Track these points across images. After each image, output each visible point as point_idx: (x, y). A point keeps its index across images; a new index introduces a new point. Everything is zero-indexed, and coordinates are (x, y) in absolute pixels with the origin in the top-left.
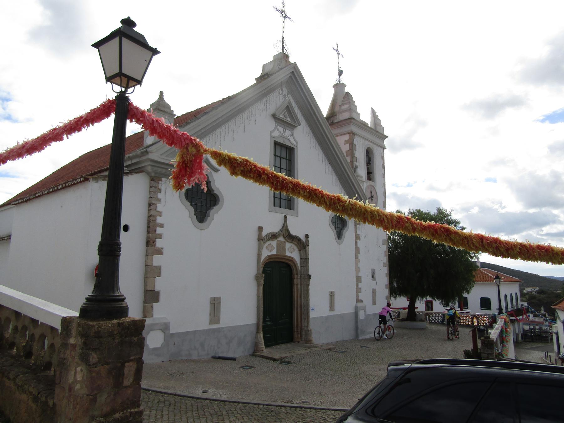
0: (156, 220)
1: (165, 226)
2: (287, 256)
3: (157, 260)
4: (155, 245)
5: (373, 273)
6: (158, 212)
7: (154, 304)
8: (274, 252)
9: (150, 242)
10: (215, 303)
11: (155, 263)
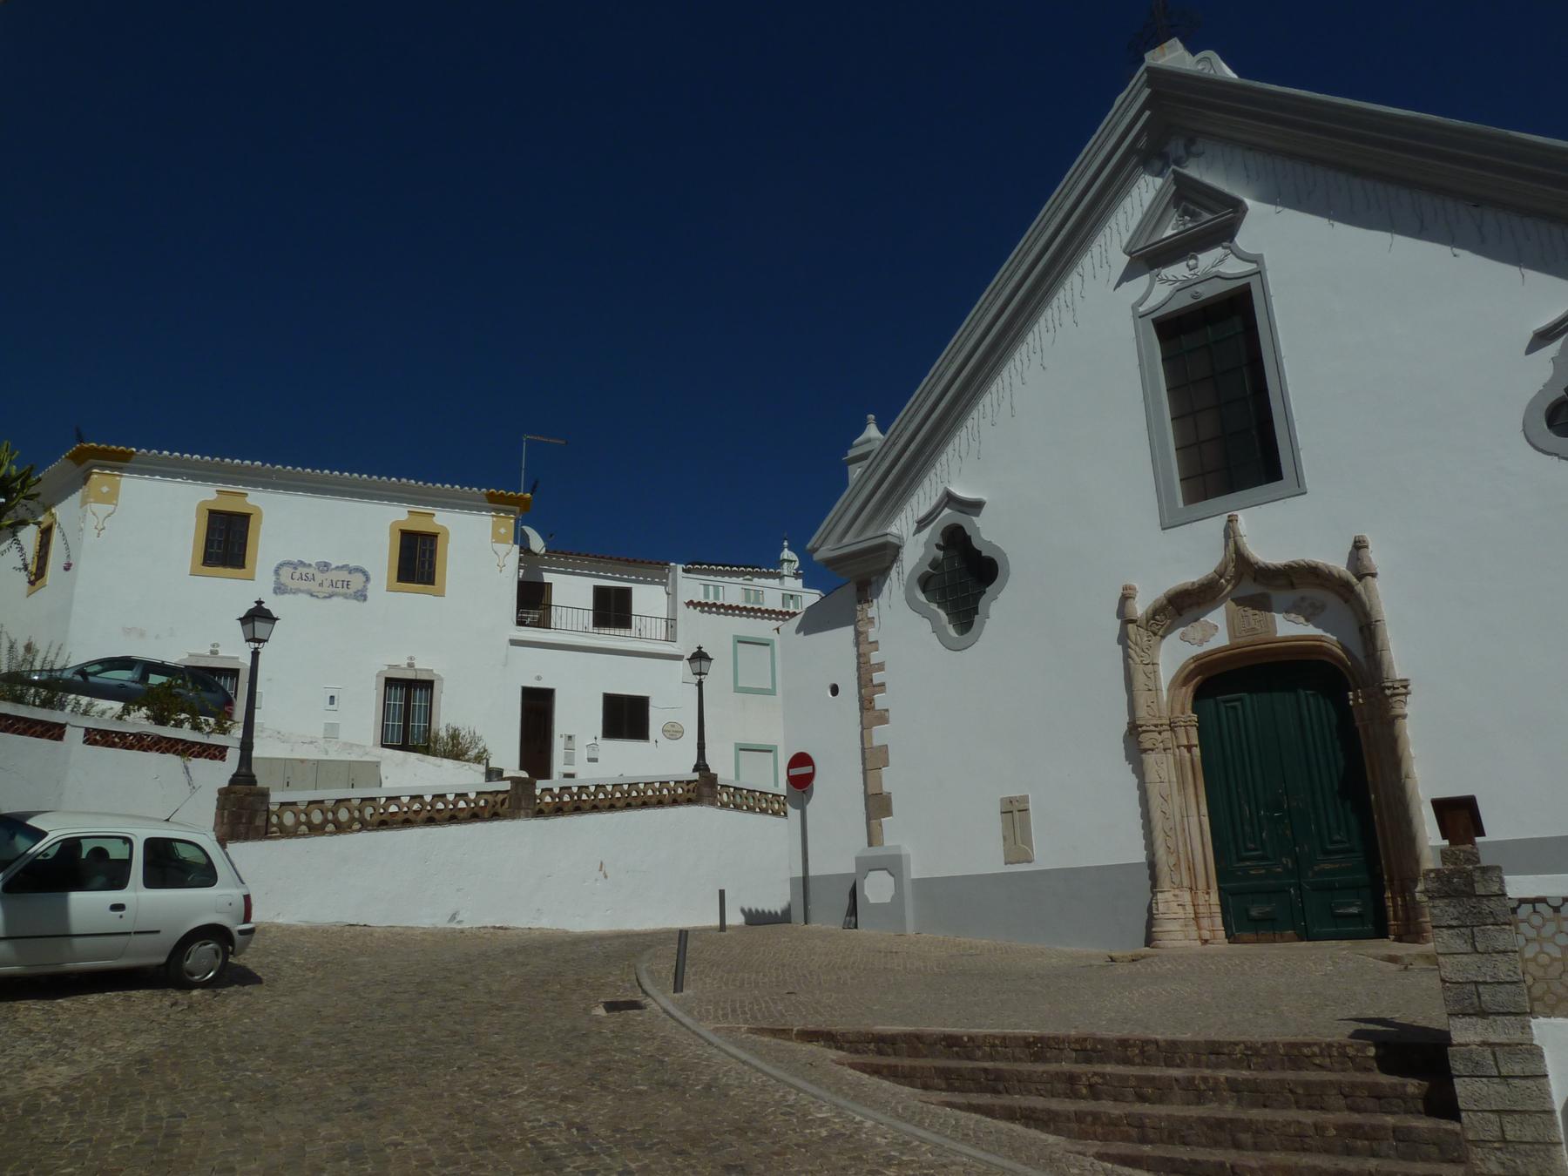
1: (886, 667)
2: (1286, 639)
3: (880, 734)
6: (871, 643)
7: (882, 819)
9: (866, 704)
10: (1015, 812)
11: (877, 742)
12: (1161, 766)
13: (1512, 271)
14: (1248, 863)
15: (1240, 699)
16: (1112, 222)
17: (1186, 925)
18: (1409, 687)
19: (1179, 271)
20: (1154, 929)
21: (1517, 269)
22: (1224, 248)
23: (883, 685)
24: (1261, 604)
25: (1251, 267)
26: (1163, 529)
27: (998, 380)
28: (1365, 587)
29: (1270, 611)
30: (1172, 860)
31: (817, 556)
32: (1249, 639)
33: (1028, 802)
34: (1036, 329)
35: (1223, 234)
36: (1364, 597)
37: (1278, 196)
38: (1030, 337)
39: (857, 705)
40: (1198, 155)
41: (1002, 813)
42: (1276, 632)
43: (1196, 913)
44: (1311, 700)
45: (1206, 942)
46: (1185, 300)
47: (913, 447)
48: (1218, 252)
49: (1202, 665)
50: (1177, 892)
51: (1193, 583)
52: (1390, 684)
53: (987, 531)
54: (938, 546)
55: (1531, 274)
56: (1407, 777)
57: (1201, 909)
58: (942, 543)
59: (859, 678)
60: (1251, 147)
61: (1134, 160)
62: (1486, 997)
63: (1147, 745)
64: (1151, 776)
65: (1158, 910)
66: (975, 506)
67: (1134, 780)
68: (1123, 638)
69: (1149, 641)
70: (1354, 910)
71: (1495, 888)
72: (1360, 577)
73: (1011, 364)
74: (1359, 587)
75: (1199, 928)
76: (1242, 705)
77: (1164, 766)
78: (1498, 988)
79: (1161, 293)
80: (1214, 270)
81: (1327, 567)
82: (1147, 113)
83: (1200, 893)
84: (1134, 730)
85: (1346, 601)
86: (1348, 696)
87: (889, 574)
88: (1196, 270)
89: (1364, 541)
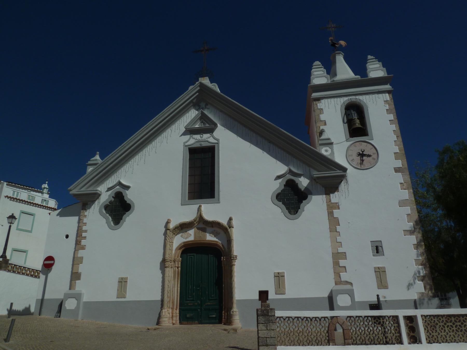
0: (82, 228)
1: (88, 232)
3: (81, 253)
4: (81, 244)
5: (377, 247)
6: (84, 223)
7: (77, 281)
8: (191, 238)
10: (123, 282)
11: (79, 255)
12: (170, 272)
13: (274, 160)
14: (188, 302)
15: (194, 255)
16: (182, 118)
17: (169, 319)
18: (237, 258)
19: (198, 137)
20: (160, 320)
21: (275, 160)
22: (210, 135)
23: (85, 237)
24: (204, 230)
25: (216, 141)
26: (181, 205)
27: (142, 153)
28: (231, 230)
29: (206, 232)
30: (168, 300)
31: (71, 192)
32: (199, 239)
33: (128, 279)
34: (156, 141)
35: (211, 131)
36: (230, 233)
37: (226, 126)
38: (153, 143)
39: (74, 242)
40: (208, 109)
41: (118, 282)
42: (206, 238)
43: (172, 316)
44: (212, 258)
45: (174, 324)
46: (198, 145)
47: (111, 165)
48: (208, 135)
49: (186, 244)
50: (168, 309)
51: (187, 222)
52: (233, 256)
53: (129, 196)
54: (113, 197)
55: (278, 162)
56: (233, 281)
57: (174, 315)
58: (114, 196)
59: (77, 234)
60: (221, 111)
61: (192, 104)
62: (268, 341)
63: (167, 266)
64: (167, 274)
65: (162, 314)
66: (128, 188)
67: (161, 276)
68: (165, 234)
69: (172, 236)
70: (214, 316)
71: (273, 314)
72: (230, 227)
73: (146, 149)
74: (229, 230)
75: (173, 320)
76: (194, 257)
77: (170, 272)
78: (271, 339)
79: (192, 141)
80: (207, 139)
81: (222, 223)
82: (197, 94)
83: (174, 310)
84: (164, 261)
85: (225, 233)
86: (221, 258)
87: (95, 202)
88: (202, 138)
89: (232, 218)
